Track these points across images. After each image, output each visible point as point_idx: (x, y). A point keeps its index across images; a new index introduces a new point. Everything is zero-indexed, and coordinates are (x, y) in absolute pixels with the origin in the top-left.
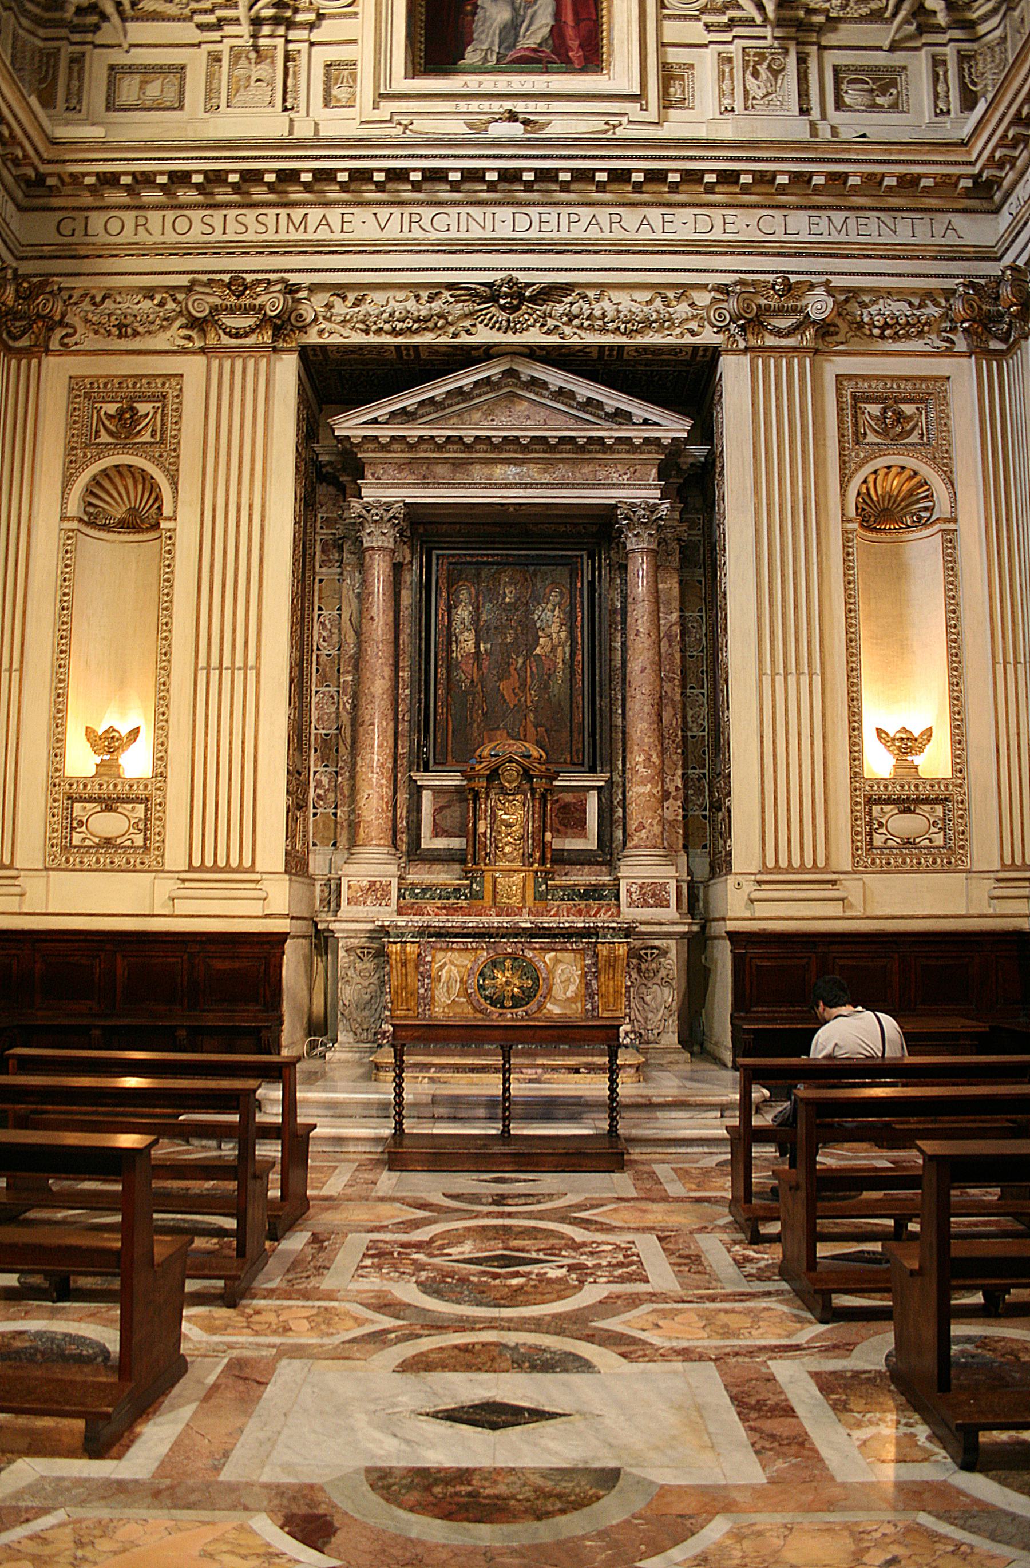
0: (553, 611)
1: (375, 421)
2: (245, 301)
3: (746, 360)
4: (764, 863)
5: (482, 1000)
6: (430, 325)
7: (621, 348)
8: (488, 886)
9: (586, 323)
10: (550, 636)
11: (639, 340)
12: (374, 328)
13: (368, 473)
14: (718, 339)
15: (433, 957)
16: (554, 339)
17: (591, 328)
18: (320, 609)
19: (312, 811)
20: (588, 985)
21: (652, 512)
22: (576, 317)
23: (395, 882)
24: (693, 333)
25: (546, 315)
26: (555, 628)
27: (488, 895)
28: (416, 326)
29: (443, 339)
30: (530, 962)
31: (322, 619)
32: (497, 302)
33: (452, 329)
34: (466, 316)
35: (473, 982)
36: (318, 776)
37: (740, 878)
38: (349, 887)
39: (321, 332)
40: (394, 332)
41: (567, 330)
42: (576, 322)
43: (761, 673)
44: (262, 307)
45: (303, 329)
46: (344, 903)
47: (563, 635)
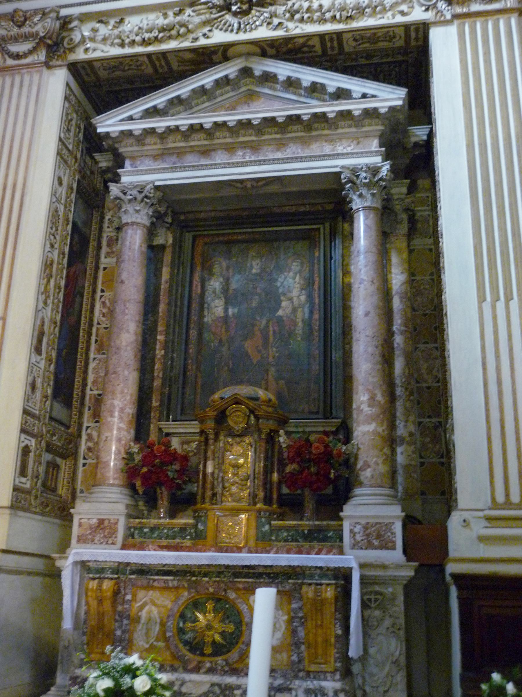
0: (294, 278)
1: (131, 118)
2: (26, 29)
3: (453, 30)
4: (493, 498)
5: (181, 646)
6: (174, 32)
7: (339, 34)
8: (211, 525)
9: (306, 16)
10: (291, 299)
11: (355, 25)
12: (127, 41)
13: (127, 163)
14: (429, 16)
15: (134, 596)
16: (280, 33)
17: (311, 20)
18: (102, 291)
19: (82, 461)
20: (294, 632)
21: (374, 175)
22: (297, 12)
23: (122, 521)
24: (403, 13)
25: (273, 15)
26: (295, 293)
27: (210, 534)
28: (161, 35)
29: (187, 44)
30: (233, 606)
31: (103, 299)
32: (229, 10)
33: (191, 36)
34: (205, 23)
35: (171, 624)
36: (89, 431)
37: (466, 515)
38: (80, 525)
39: (86, 50)
40: (145, 42)
41: (291, 25)
42: (297, 16)
43: (482, 299)
44: (37, 33)
45: (72, 50)
46: (74, 541)
47: (303, 298)
